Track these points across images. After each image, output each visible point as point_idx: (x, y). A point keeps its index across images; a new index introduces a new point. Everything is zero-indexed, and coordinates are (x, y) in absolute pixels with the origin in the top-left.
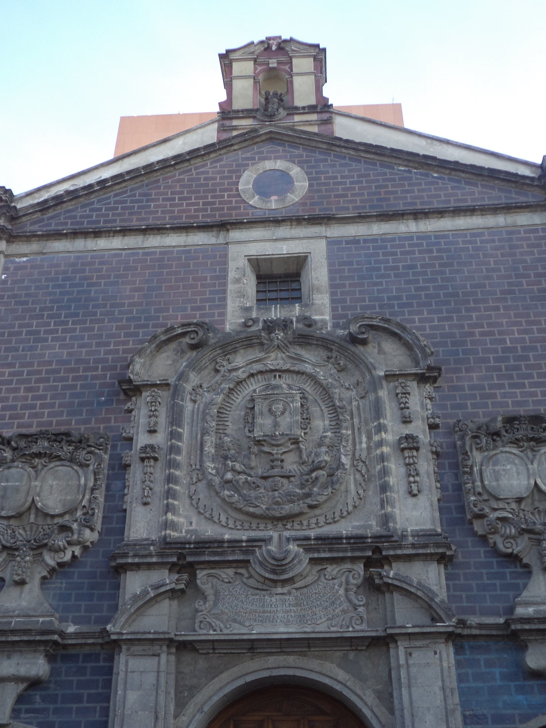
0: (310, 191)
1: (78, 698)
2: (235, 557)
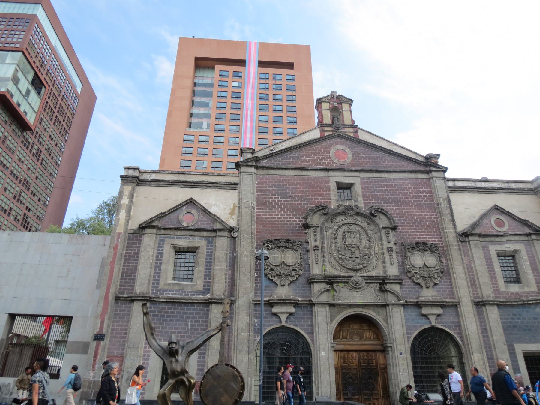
0: (353, 159)
1: (303, 318)
2: (346, 280)
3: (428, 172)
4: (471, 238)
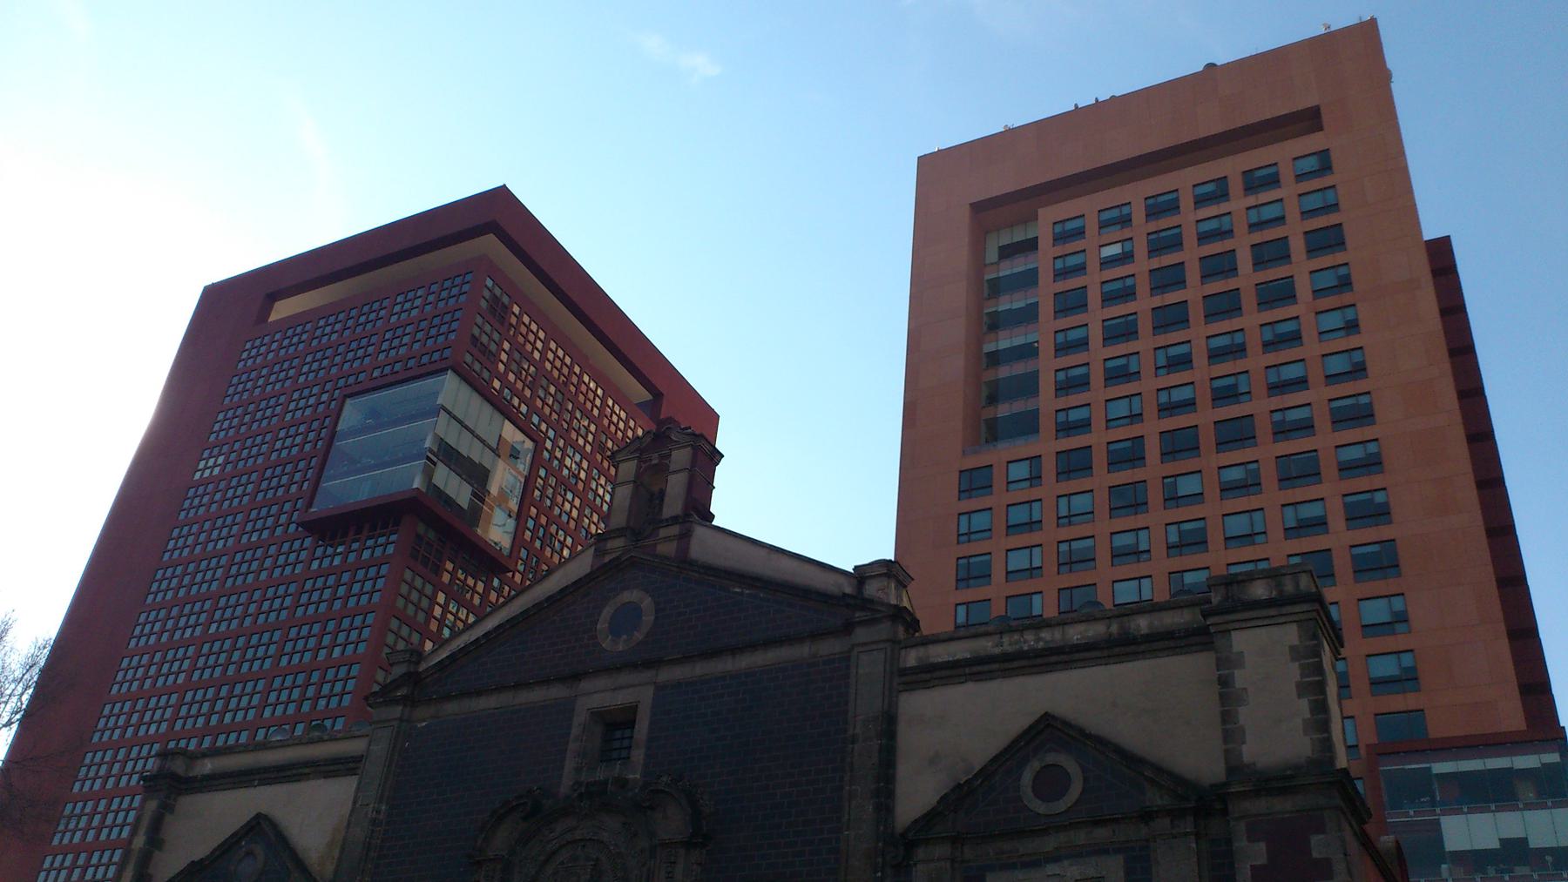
3: (848, 628)
4: (921, 853)
